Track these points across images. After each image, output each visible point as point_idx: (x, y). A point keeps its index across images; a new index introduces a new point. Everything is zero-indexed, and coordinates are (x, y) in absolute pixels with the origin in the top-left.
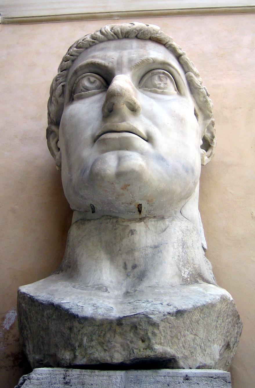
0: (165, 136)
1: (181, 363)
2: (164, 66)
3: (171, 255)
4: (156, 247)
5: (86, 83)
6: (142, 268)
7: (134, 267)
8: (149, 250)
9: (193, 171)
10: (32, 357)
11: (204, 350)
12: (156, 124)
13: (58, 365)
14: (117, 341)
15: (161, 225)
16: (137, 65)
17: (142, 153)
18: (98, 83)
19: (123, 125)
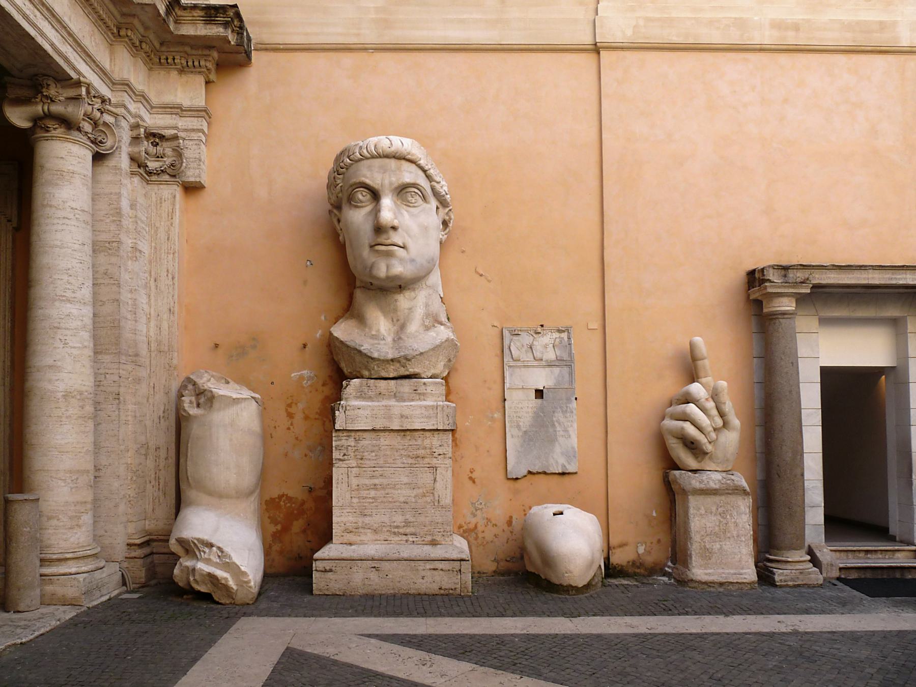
0: (415, 230)
1: (423, 376)
2: (414, 185)
3: (419, 312)
4: (410, 309)
5: (360, 197)
6: (402, 321)
7: (398, 320)
8: (406, 311)
9: (433, 259)
10: (346, 371)
11: (434, 367)
12: (409, 236)
13: (362, 377)
14: (391, 367)
15: (413, 294)
16: (396, 188)
17: (402, 260)
18: (369, 196)
19: (389, 242)
